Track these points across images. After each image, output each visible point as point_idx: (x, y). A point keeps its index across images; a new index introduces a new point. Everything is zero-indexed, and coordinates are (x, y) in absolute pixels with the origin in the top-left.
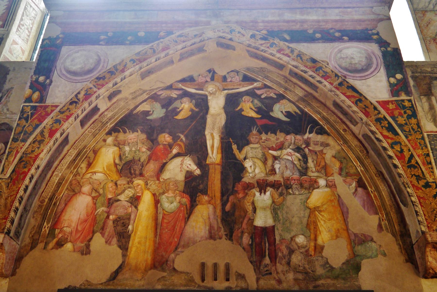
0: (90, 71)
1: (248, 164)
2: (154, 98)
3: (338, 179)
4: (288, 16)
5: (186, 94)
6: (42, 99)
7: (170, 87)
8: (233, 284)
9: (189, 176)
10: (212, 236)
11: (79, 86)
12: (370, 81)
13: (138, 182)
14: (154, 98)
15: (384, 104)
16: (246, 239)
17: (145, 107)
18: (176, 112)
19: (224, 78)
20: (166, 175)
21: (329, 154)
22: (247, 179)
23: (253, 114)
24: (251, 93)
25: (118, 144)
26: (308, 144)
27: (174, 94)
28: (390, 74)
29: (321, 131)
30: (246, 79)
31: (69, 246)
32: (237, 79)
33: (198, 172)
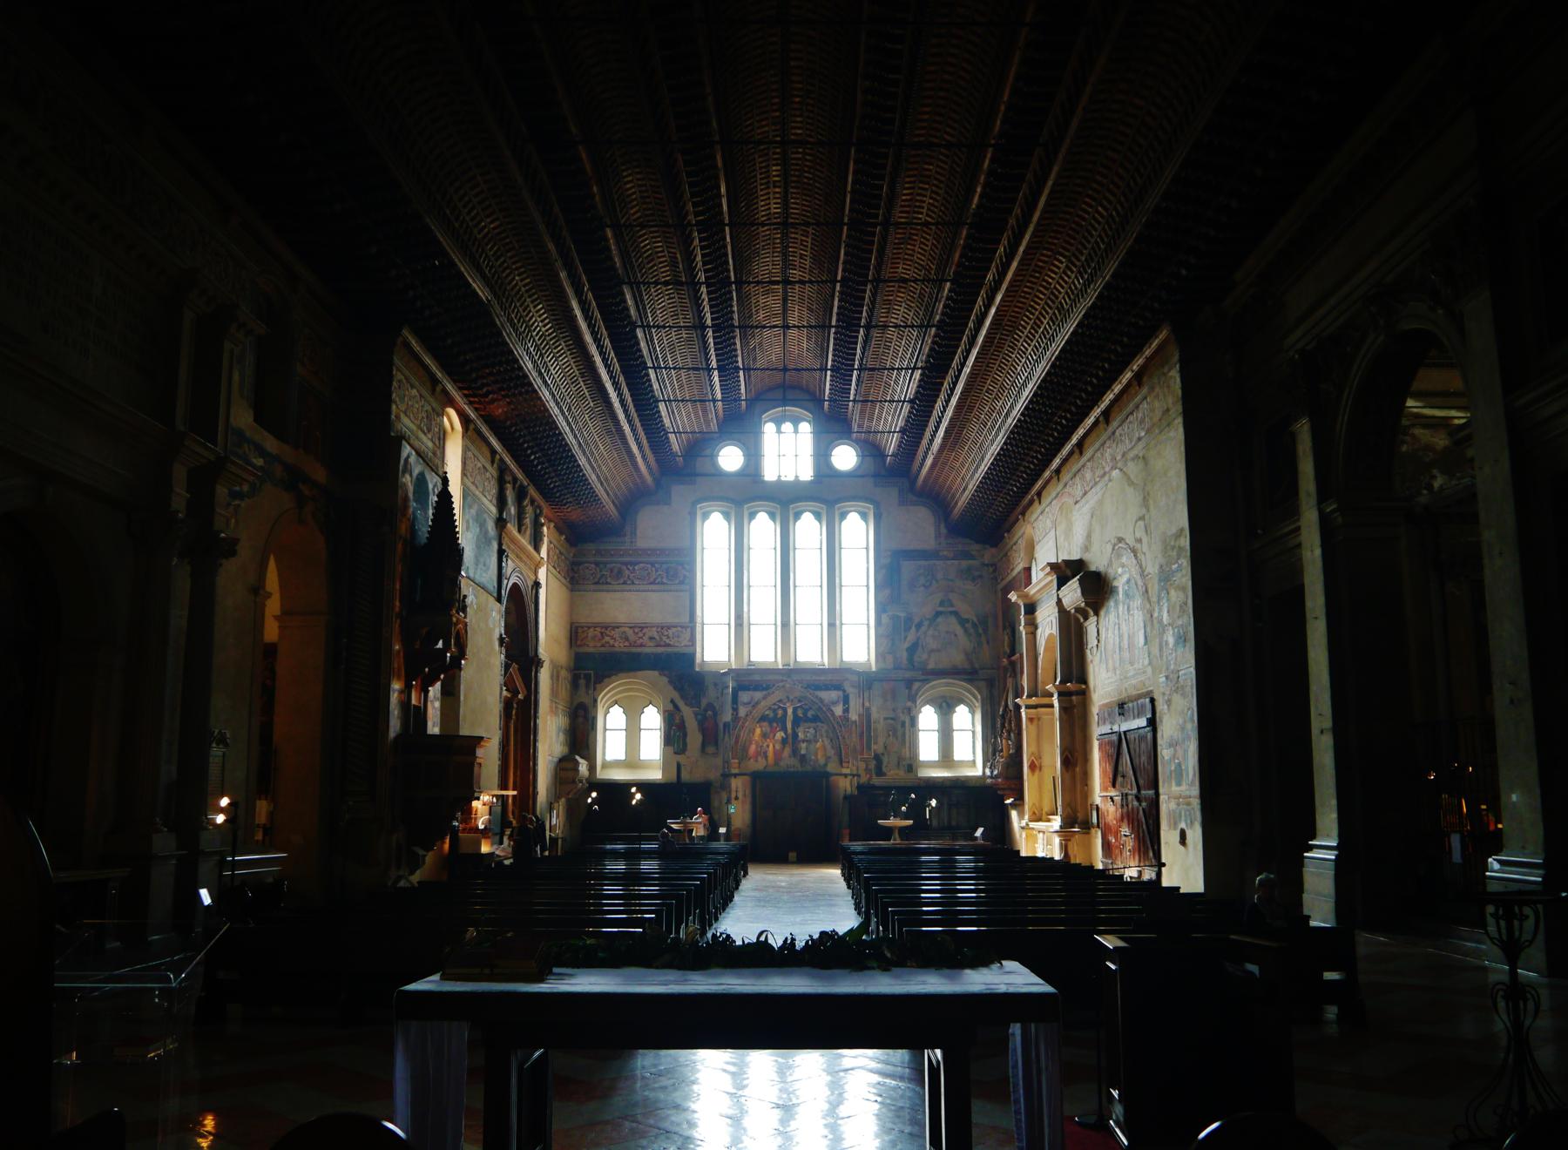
0: (749, 703)
1: (800, 734)
2: (770, 708)
3: (825, 739)
4: (814, 678)
5: (780, 707)
6: (737, 714)
7: (775, 704)
8: (796, 770)
9: (782, 737)
10: (790, 757)
11: (747, 709)
12: (837, 708)
13: (768, 740)
14: (770, 708)
15: (840, 717)
16: (799, 757)
17: (767, 713)
18: (777, 714)
19: (792, 701)
20: (776, 738)
21: (823, 730)
22: (799, 739)
23: (801, 715)
24: (800, 707)
25: (761, 727)
26: (817, 726)
27: (776, 707)
28: (844, 705)
29: (822, 722)
30: (799, 701)
31: (752, 760)
32: (796, 701)
33: (784, 736)
